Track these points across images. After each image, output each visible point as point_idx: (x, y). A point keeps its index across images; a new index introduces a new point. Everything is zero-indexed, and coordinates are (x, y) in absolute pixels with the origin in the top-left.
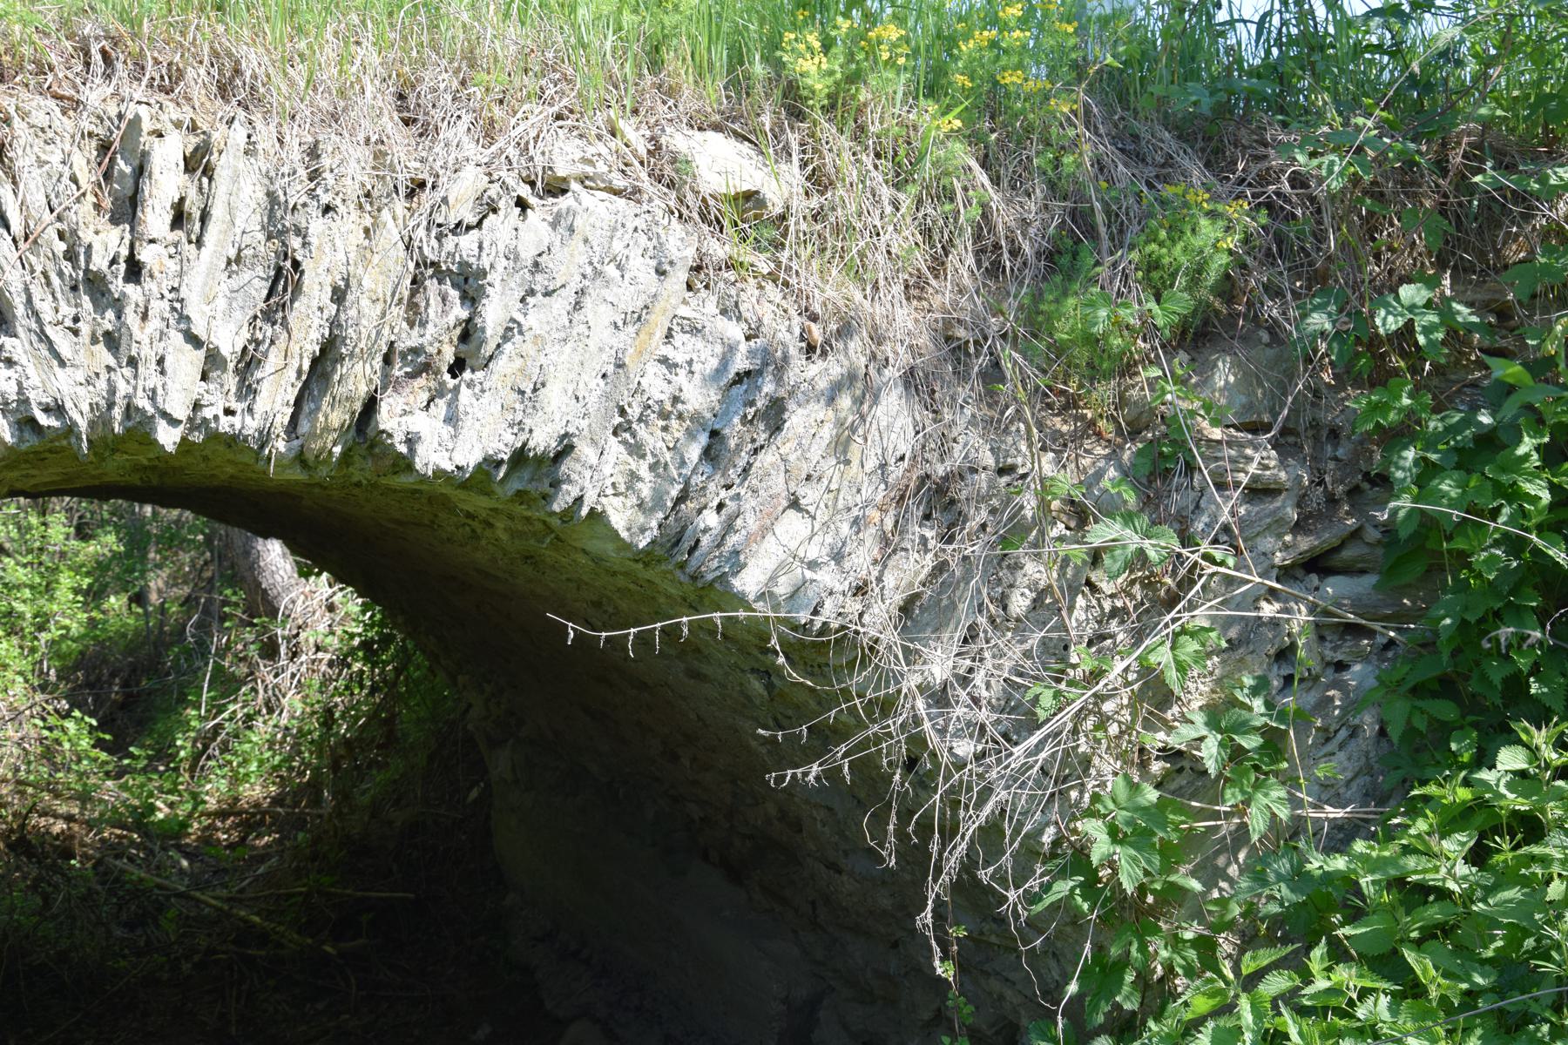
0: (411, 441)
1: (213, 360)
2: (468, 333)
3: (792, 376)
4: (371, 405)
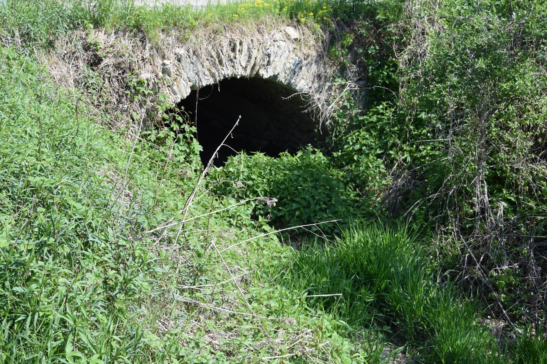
0: (263, 75)
1: (243, 67)
2: (269, 61)
3: (303, 63)
4: (258, 71)
